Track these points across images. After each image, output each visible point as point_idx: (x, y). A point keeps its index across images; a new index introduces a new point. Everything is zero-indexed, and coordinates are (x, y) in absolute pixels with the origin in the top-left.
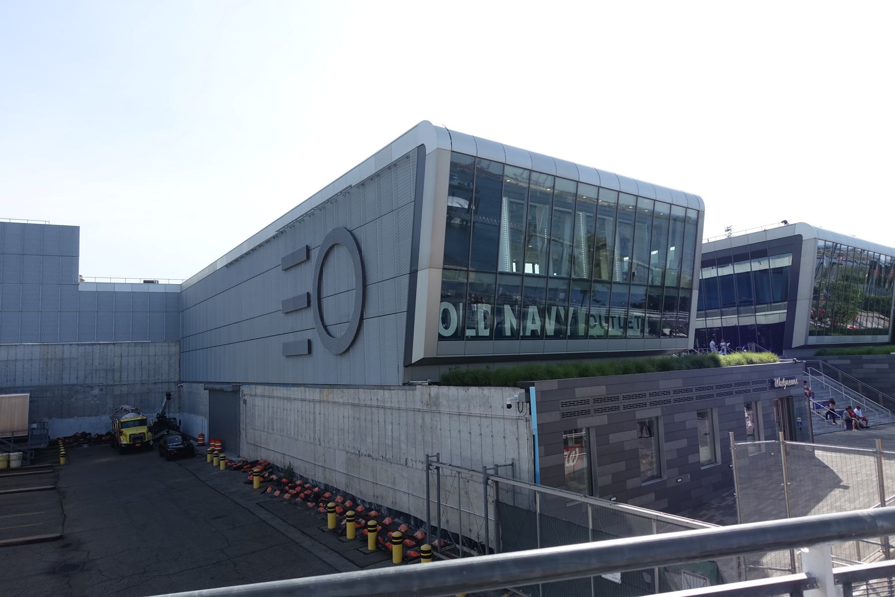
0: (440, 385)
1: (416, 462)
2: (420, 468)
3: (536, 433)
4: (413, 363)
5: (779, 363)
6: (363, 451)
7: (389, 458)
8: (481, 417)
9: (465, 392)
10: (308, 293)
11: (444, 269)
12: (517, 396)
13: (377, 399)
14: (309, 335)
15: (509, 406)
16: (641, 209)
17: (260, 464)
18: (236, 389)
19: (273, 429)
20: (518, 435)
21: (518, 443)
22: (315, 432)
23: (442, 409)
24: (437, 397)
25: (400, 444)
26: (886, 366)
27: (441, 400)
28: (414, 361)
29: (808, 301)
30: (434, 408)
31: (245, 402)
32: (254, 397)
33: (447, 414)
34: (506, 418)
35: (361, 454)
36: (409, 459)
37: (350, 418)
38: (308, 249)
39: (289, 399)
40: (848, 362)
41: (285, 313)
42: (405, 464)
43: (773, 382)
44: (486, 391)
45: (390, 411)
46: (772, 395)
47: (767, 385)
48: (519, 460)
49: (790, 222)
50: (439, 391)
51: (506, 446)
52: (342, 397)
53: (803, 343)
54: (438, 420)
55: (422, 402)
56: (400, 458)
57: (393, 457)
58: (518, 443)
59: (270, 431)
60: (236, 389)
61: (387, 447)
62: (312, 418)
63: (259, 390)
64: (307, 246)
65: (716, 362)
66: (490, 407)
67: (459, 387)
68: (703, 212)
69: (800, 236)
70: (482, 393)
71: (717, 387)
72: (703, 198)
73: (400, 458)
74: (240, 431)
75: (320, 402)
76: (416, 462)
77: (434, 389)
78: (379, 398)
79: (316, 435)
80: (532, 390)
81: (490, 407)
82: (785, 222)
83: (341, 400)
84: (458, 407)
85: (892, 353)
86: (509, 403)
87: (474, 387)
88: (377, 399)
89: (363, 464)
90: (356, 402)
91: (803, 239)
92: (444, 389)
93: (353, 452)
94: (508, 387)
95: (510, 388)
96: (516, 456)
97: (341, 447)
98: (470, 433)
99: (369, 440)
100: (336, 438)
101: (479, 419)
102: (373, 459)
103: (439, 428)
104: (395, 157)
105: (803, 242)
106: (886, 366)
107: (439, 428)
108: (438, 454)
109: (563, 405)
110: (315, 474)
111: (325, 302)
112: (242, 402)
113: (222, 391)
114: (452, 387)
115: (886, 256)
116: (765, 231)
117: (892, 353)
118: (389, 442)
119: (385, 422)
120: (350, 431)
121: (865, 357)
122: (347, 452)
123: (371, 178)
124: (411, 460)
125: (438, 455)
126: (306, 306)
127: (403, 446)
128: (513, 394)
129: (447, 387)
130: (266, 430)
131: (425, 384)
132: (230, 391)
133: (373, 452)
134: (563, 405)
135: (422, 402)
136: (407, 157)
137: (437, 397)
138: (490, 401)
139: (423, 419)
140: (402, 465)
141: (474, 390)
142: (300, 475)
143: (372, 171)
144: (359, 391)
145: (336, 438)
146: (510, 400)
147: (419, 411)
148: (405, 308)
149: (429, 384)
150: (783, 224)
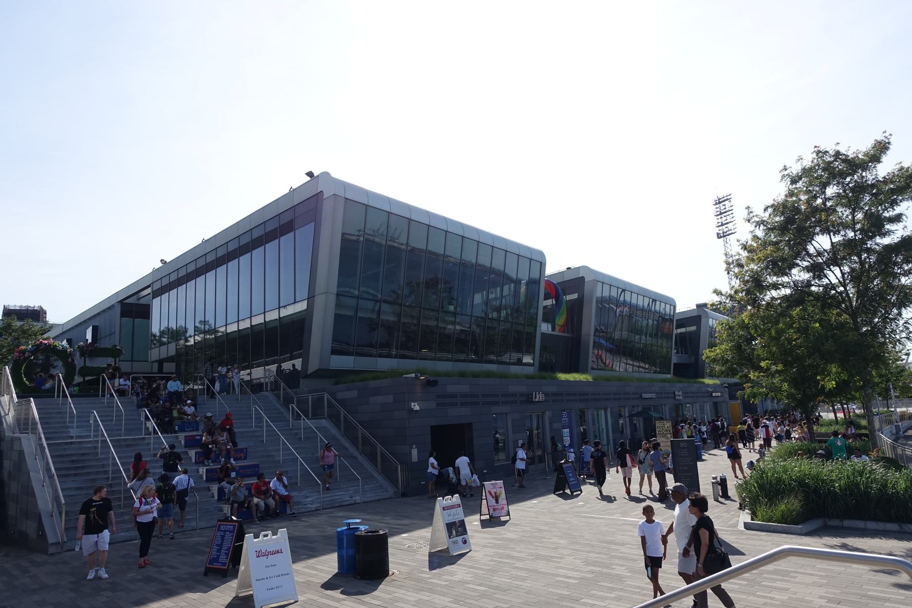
69: (583, 278)
91: (586, 281)
115: (666, 304)
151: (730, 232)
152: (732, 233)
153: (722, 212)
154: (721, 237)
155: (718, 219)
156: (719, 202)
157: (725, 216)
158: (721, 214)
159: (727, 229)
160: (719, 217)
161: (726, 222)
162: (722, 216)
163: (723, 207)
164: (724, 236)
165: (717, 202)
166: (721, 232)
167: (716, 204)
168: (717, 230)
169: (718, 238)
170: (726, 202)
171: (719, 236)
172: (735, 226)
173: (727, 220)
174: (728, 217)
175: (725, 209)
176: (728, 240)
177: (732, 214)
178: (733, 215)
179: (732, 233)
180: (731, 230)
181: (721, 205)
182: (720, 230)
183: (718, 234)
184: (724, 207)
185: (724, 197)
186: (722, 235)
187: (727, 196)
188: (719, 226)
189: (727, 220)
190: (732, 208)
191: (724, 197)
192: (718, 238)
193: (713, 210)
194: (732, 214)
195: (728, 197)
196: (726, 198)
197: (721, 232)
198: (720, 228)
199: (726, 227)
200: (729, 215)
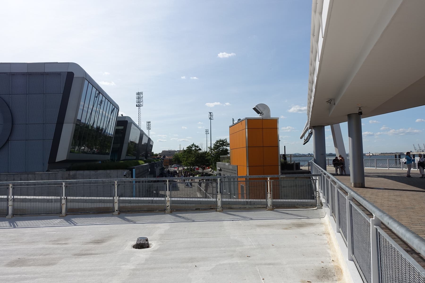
4: (56, 162)
9: (95, 172)
15: (125, 176)
44: (108, 171)
66: (110, 177)
69: (127, 121)
80: (134, 170)
81: (110, 177)
82: (122, 115)
86: (125, 174)
95: (122, 170)
105: (128, 123)
123: (23, 74)
131: (64, 170)
138: (110, 175)
149: (66, 170)
150: (121, 116)
151: (141, 105)
152: (142, 106)
154: (137, 106)
155: (137, 100)
156: (138, 94)
157: (140, 99)
158: (139, 98)
159: (140, 104)
161: (140, 101)
164: (139, 106)
165: (138, 94)
166: (138, 104)
167: (137, 94)
169: (137, 106)
170: (141, 95)
171: (137, 106)
173: (140, 101)
174: (141, 100)
175: (140, 97)
176: (140, 108)
179: (142, 106)
180: (141, 105)
182: (137, 104)
183: (137, 105)
186: (138, 106)
188: (137, 102)
189: (140, 101)
191: (140, 93)
192: (137, 106)
194: (142, 99)
195: (142, 93)
196: (141, 93)
197: (138, 104)
198: (138, 103)
199: (140, 103)
200: (141, 99)
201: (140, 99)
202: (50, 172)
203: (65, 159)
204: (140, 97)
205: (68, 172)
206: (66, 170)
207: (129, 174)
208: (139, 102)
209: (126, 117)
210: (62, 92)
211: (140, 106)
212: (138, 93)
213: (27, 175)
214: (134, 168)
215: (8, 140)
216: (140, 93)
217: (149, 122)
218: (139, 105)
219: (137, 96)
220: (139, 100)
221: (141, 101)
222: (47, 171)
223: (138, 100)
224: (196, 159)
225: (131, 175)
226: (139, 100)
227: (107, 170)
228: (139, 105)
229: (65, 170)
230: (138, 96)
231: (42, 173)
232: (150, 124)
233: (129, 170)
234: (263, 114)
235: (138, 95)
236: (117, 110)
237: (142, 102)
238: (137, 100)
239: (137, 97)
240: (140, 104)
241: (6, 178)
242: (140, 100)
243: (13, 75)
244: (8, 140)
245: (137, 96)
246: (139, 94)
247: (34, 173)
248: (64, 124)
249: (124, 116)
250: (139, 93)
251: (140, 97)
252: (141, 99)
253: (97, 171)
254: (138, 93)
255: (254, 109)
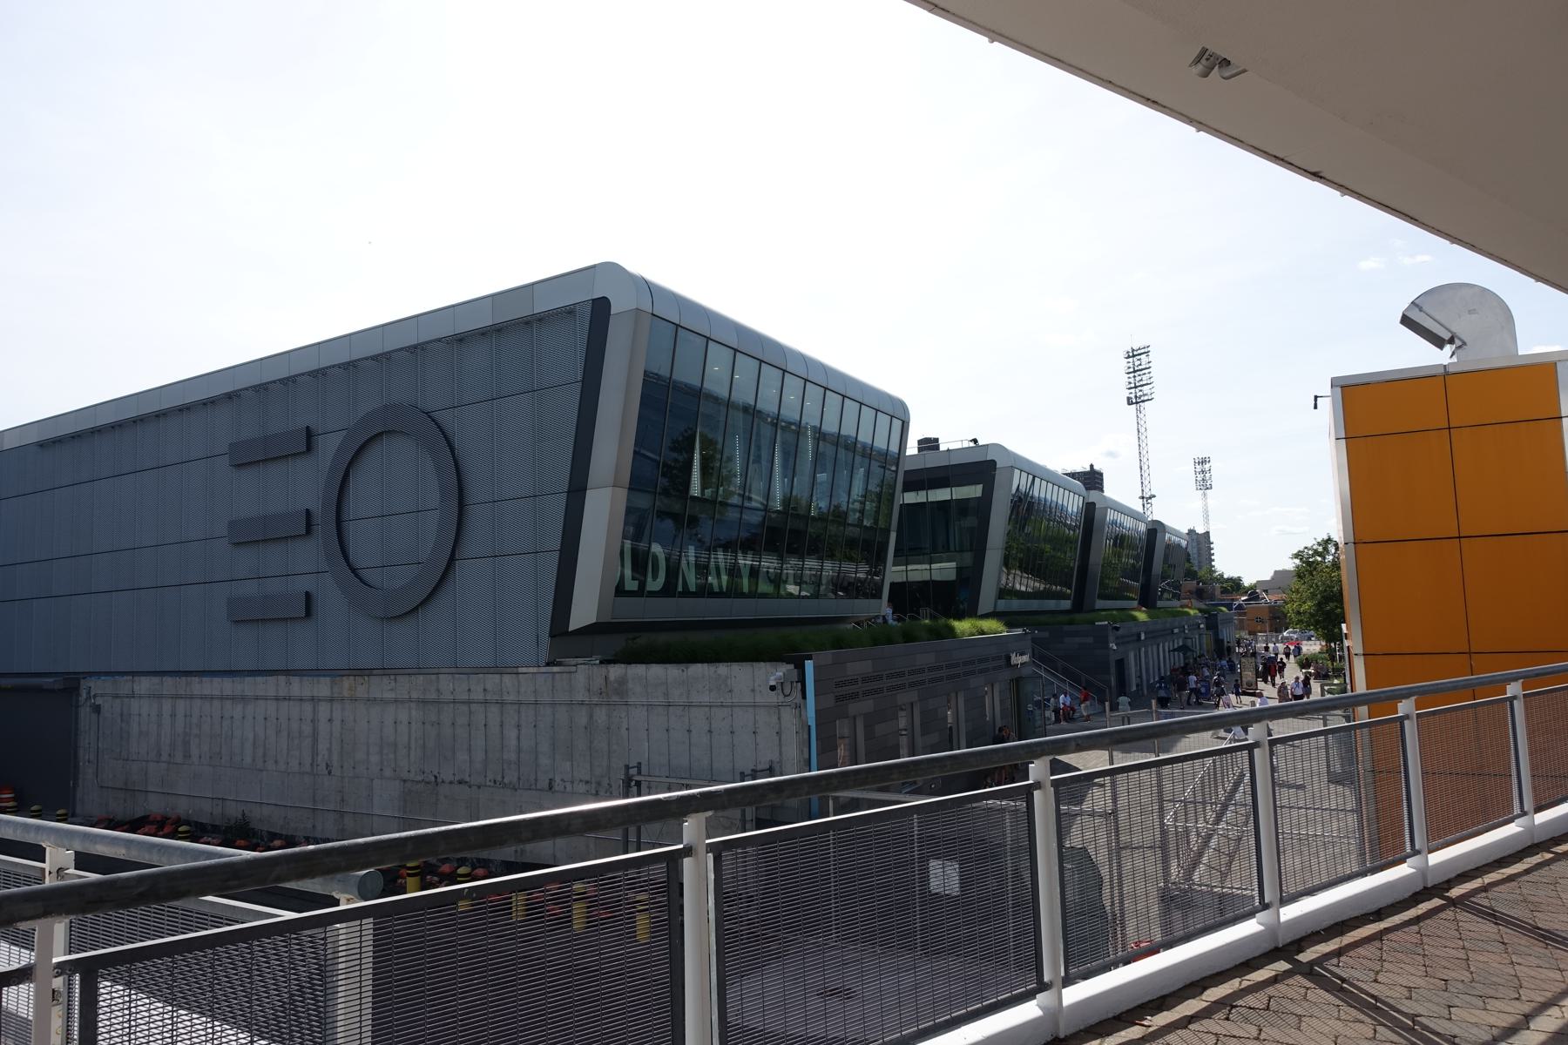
0: (630, 664)
1: (572, 782)
2: (581, 791)
3: (812, 723)
4: (570, 630)
5: (1006, 634)
6: (447, 775)
7: (510, 783)
8: (710, 706)
9: (680, 671)
10: (308, 512)
11: (629, 489)
12: (781, 674)
13: (485, 690)
14: (303, 584)
15: (773, 688)
16: (705, 389)
17: (152, 823)
18: (70, 686)
19: (187, 756)
20: (780, 728)
21: (780, 740)
22: (315, 753)
23: (632, 700)
24: (622, 681)
25: (536, 758)
26: (1090, 640)
27: (630, 685)
28: (574, 625)
29: (1000, 551)
30: (615, 698)
31: (97, 709)
32: (126, 700)
33: (643, 705)
34: (759, 706)
35: (439, 780)
36: (558, 779)
37: (413, 724)
38: (309, 434)
39: (243, 699)
40: (1046, 634)
41: (234, 544)
42: (547, 786)
43: (1009, 658)
44: (722, 669)
45: (516, 707)
46: (1006, 675)
47: (1002, 662)
48: (780, 762)
49: (981, 443)
50: (626, 672)
51: (757, 744)
52: (392, 690)
53: (991, 610)
54: (623, 716)
55: (589, 690)
56: (536, 780)
57: (519, 779)
58: (780, 740)
59: (179, 758)
60: (70, 686)
61: (505, 767)
62: (307, 729)
63: (144, 685)
64: (308, 427)
65: (951, 632)
66: (730, 691)
67: (668, 665)
68: (909, 423)
69: (993, 462)
70: (715, 672)
71: (910, 673)
72: (910, 409)
73: (536, 780)
74: (76, 767)
75: (331, 700)
76: (572, 782)
77: (616, 671)
78: (489, 687)
79: (320, 758)
80: (809, 664)
81: (730, 691)
82: (975, 441)
83: (389, 695)
84: (666, 695)
85: (1097, 623)
86: (773, 683)
87: (699, 665)
88: (485, 690)
89: (446, 797)
90: (432, 696)
92: (638, 670)
93: (420, 779)
94: (764, 661)
95: (768, 664)
96: (775, 757)
97: (388, 772)
98: (689, 731)
99: (462, 756)
100: (374, 759)
101: (707, 709)
102: (470, 787)
103: (625, 726)
104: (541, 307)
106: (1090, 640)
107: (625, 726)
108: (640, 763)
109: (838, 685)
110: (314, 826)
111: (351, 529)
112: (85, 713)
113: (39, 690)
114: (654, 665)
116: (948, 450)
117: (1097, 623)
118: (513, 757)
119: (501, 726)
120: (413, 746)
121: (1066, 628)
122: (405, 781)
123: (483, 333)
124: (562, 780)
125: (639, 766)
126: (304, 532)
127: (544, 761)
128: (778, 672)
129: (644, 666)
130: (165, 757)
131: (594, 662)
132: (59, 690)
133: (470, 776)
134: (838, 685)
135: (589, 690)
136: (569, 312)
137: (622, 681)
139: (591, 717)
140: (540, 790)
141: (697, 669)
142: (268, 832)
143: (486, 321)
144: (438, 678)
145: (374, 759)
146: (775, 679)
147: (582, 703)
148: (556, 543)
149: (601, 662)
150: (972, 444)
151: (1146, 398)
152: (1149, 400)
153: (1136, 369)
154: (1132, 403)
155: (1129, 378)
156: (1132, 354)
157: (1139, 375)
158: (1135, 371)
159: (1141, 393)
160: (1132, 375)
161: (1141, 383)
162: (1136, 374)
163: (1137, 363)
164: (1137, 403)
165: (1131, 354)
166: (1133, 396)
167: (1129, 357)
168: (1126, 393)
169: (1129, 404)
170: (1143, 357)
171: (1130, 402)
172: (1153, 391)
173: (1141, 380)
174: (1144, 377)
175: (1140, 365)
177: (1149, 373)
178: (1151, 375)
179: (1149, 400)
181: (1135, 359)
183: (1129, 398)
184: (1139, 362)
185: (1139, 349)
186: (1134, 401)
187: (1144, 348)
189: (1141, 380)
190: (1150, 365)
191: (1139, 349)
192: (1129, 404)
193: (1123, 364)
194: (1149, 373)
195: (1146, 350)
196: (1143, 351)
197: (1133, 396)
198: (1133, 391)
199: (1141, 391)
200: (1145, 374)
201: (1141, 373)
202: (555, 669)
203: (594, 621)
204: (1140, 365)
205: (603, 670)
206: (601, 662)
207: (792, 682)
208: (1136, 387)
209: (988, 445)
210: (580, 378)
211: (1143, 401)
212: (1133, 350)
213: (497, 676)
214: (810, 658)
215: (452, 559)
216: (1139, 352)
217: (1203, 461)
218: (1136, 397)
219: (1129, 362)
220: (1138, 379)
221: (1144, 382)
222: (548, 664)
223: (1132, 380)
224: (1319, 605)
225: (799, 684)
226: (1138, 379)
227: (717, 664)
228: (1140, 398)
229: (598, 662)
230: (1131, 365)
231: (534, 670)
232: (1207, 467)
233: (791, 667)
234: (1464, 343)
235: (1131, 360)
236: (897, 424)
237: (1148, 384)
238: (1129, 378)
239: (1129, 368)
240: (1141, 393)
241: (451, 685)
242: (1140, 378)
243: (461, 339)
244: (452, 559)
245: (1129, 362)
246: (1134, 356)
247: (515, 670)
248: (588, 491)
249: (981, 443)
250: (1135, 353)
251: (1140, 367)
252: (1144, 372)
253: (687, 668)
254: (1133, 350)
255: (1406, 321)
